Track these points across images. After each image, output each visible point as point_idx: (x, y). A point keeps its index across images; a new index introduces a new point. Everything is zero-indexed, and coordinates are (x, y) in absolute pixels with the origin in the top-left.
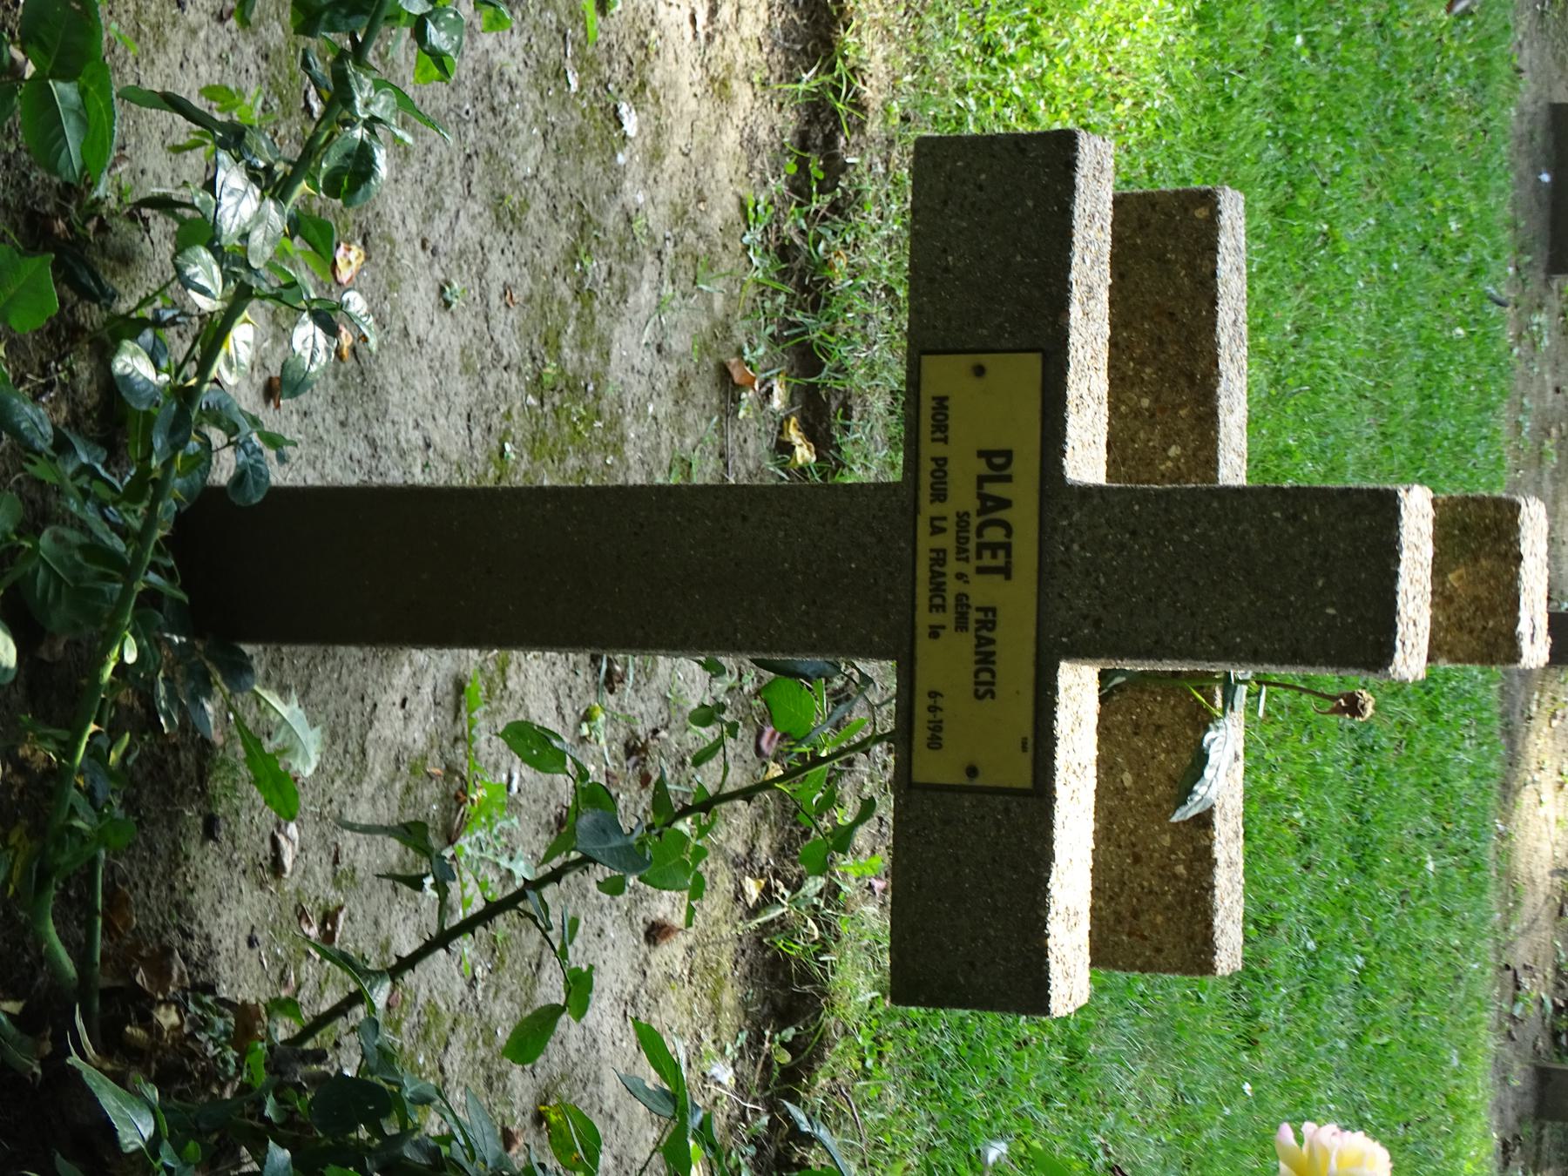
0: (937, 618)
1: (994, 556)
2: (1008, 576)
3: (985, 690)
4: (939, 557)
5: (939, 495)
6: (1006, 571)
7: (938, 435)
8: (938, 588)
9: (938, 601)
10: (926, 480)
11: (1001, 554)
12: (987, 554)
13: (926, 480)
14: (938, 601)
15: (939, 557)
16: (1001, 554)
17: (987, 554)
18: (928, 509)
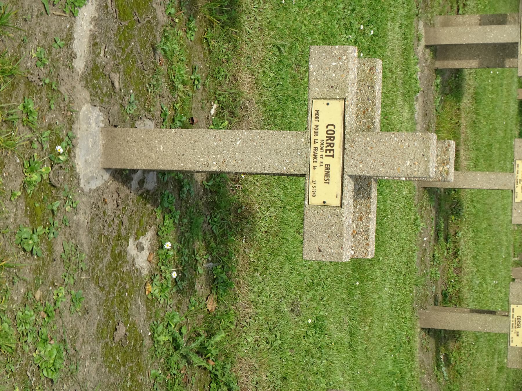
0: (315, 164)
1: (330, 152)
2: (333, 157)
3: (327, 181)
4: (316, 149)
5: (316, 134)
6: (333, 156)
7: (317, 120)
8: (315, 157)
9: (315, 160)
10: (313, 131)
11: (332, 152)
12: (328, 152)
13: (313, 131)
14: (315, 160)
15: (316, 149)
16: (332, 152)
17: (328, 152)
18: (313, 137)
